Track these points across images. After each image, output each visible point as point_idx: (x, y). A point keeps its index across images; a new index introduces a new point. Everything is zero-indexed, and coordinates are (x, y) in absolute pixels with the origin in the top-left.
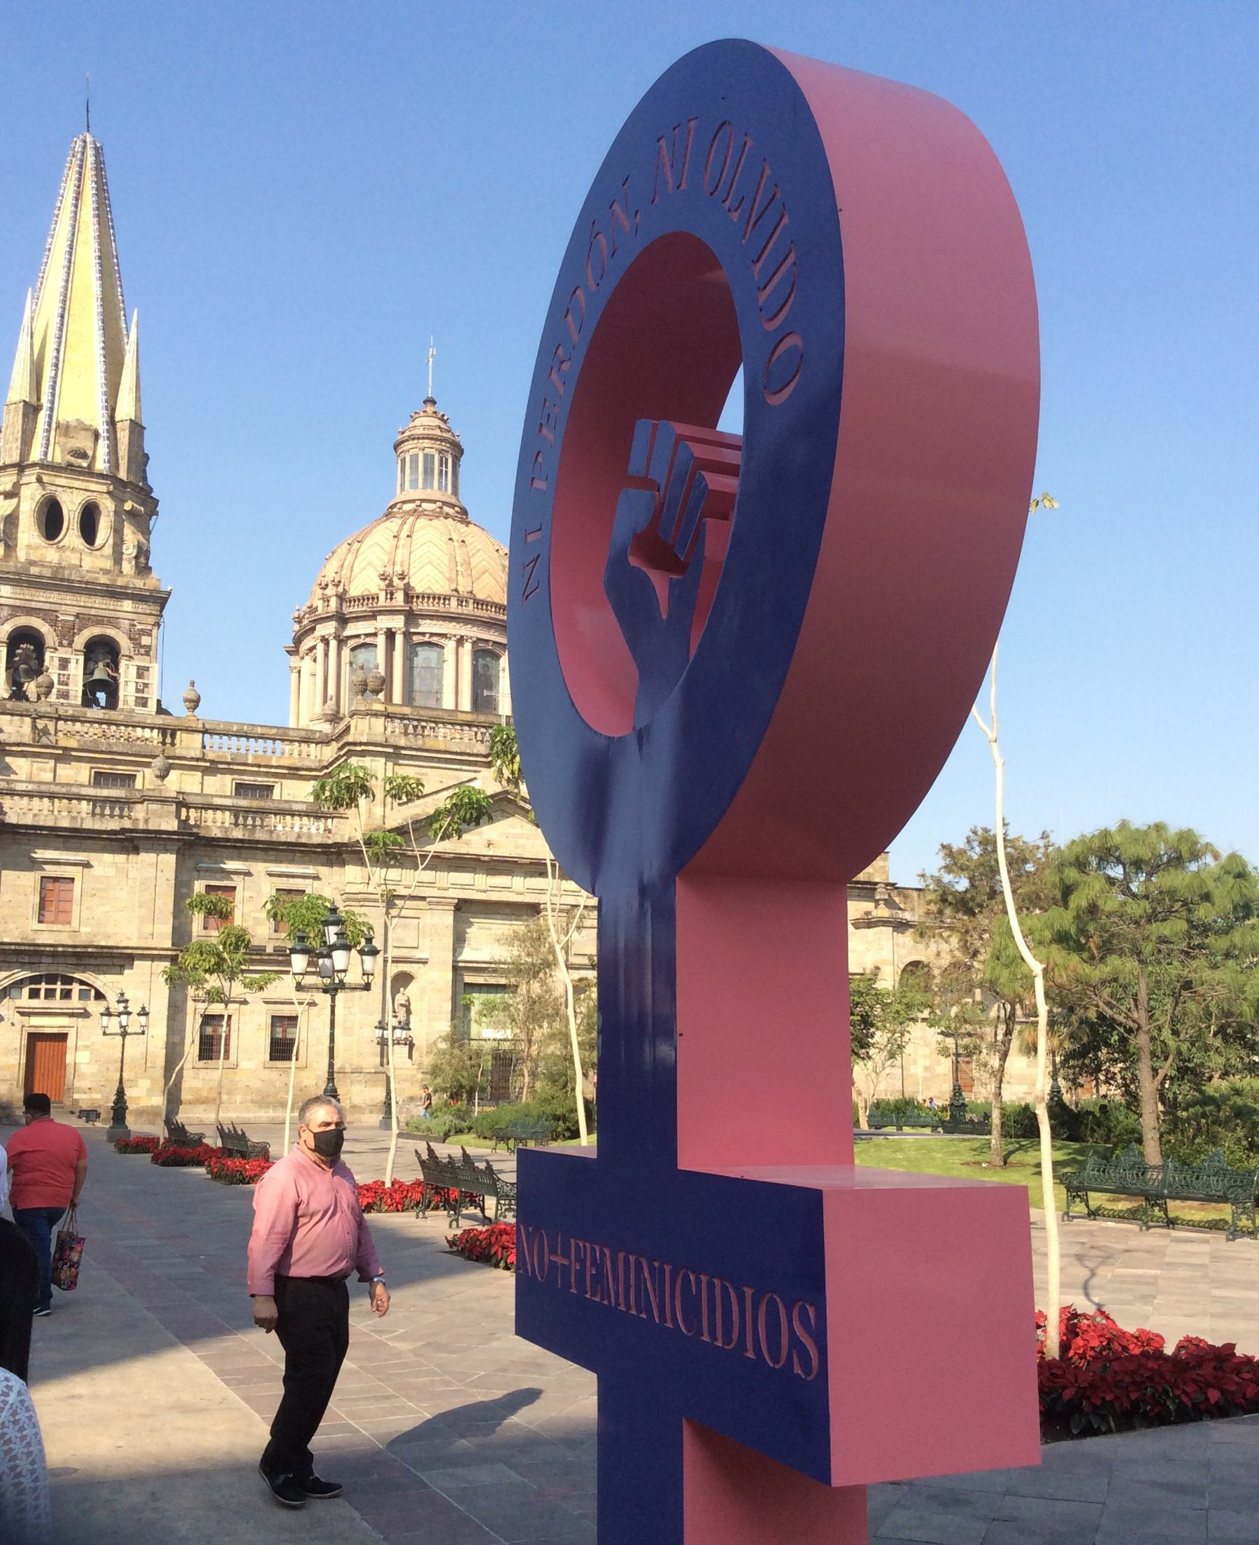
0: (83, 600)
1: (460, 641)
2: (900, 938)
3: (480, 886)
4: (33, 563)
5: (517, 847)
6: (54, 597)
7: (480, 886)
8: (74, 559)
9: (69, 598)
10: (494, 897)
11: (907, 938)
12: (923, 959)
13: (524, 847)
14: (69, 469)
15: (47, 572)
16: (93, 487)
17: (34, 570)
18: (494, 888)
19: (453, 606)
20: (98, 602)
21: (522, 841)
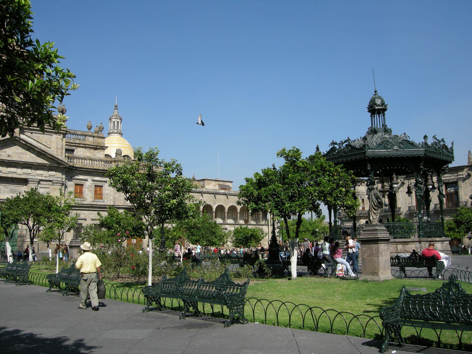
5: (19, 157)
10: (10, 175)
13: (22, 157)
18: (10, 172)
21: (21, 155)
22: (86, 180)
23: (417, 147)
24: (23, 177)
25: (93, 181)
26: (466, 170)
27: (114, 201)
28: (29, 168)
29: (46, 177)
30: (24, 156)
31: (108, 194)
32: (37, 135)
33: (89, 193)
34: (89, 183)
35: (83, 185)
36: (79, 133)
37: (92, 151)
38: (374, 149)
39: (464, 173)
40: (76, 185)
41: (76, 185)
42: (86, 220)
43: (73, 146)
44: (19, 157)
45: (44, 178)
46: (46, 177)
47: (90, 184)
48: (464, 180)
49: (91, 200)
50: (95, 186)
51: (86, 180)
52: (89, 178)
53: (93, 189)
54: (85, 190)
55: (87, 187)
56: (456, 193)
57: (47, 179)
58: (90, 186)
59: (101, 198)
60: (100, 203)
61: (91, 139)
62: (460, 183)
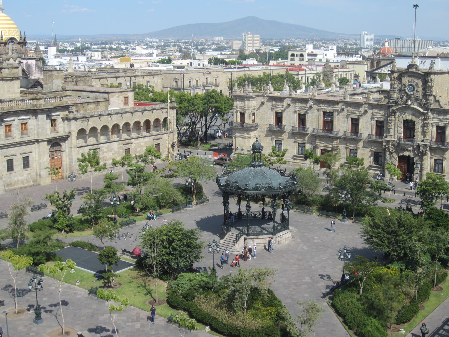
2: (77, 123)
11: (79, 122)
12: (83, 128)
22: (14, 120)
23: (275, 190)
25: (19, 120)
26: (341, 104)
27: (38, 135)
31: (31, 129)
33: (17, 130)
34: (16, 122)
35: (11, 125)
37: (9, 82)
38: (251, 190)
39: (339, 107)
40: (6, 126)
41: (6, 126)
42: (16, 155)
47: (17, 123)
48: (339, 113)
49: (19, 137)
50: (22, 124)
51: (14, 120)
52: (16, 118)
53: (20, 127)
54: (13, 129)
56: (332, 122)
58: (17, 125)
59: (26, 134)
60: (27, 139)
61: (6, 71)
62: (335, 114)
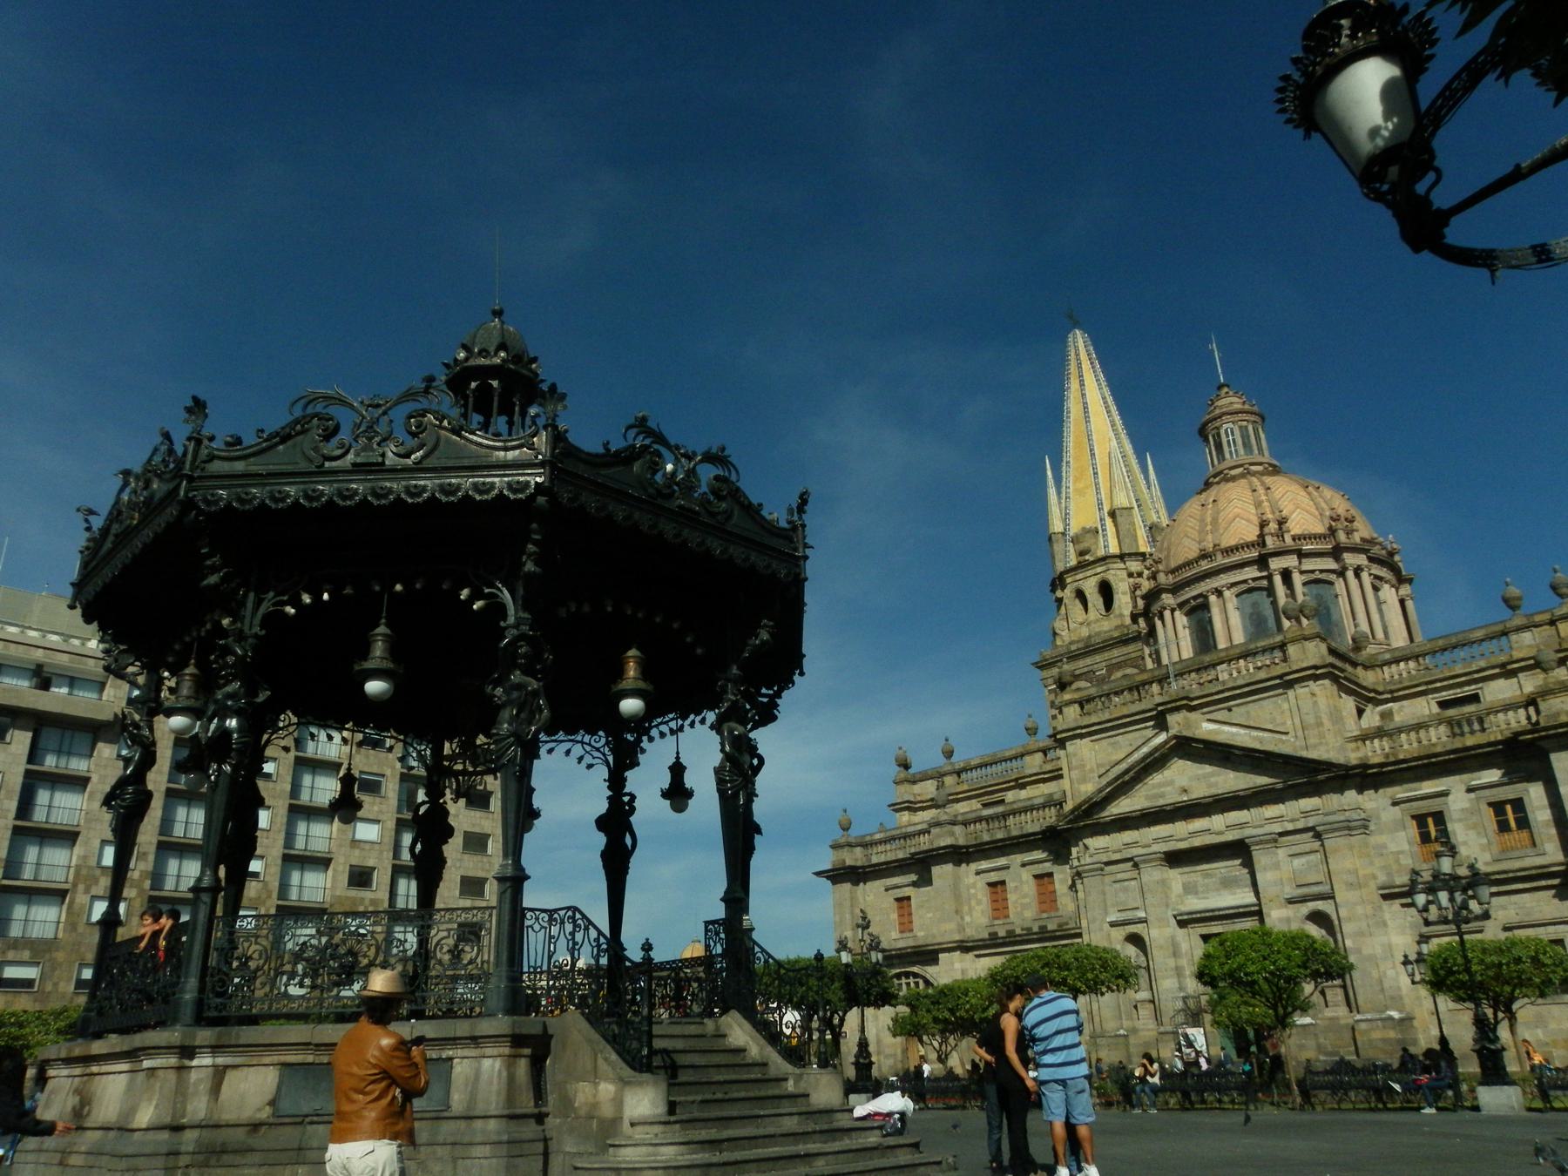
0: (1107, 655)
1: (1219, 593)
3: (1183, 833)
4: (1072, 643)
5: (1210, 786)
6: (1088, 661)
7: (1183, 833)
8: (1096, 628)
9: (1098, 658)
10: (1197, 842)
13: (1216, 784)
14: (1081, 566)
15: (1081, 645)
16: (1099, 570)
17: (1073, 648)
18: (1193, 834)
19: (1205, 565)
20: (1115, 652)
22: (1445, 794)
24: (1230, 836)
28: (1240, 808)
29: (1292, 821)
30: (1220, 779)
32: (1243, 709)
33: (1472, 834)
36: (1479, 634)
43: (1468, 683)
44: (1210, 786)
45: (1290, 827)
46: (1292, 821)
47: (1467, 805)
55: (1455, 816)
57: (1300, 825)
58: (1470, 812)
